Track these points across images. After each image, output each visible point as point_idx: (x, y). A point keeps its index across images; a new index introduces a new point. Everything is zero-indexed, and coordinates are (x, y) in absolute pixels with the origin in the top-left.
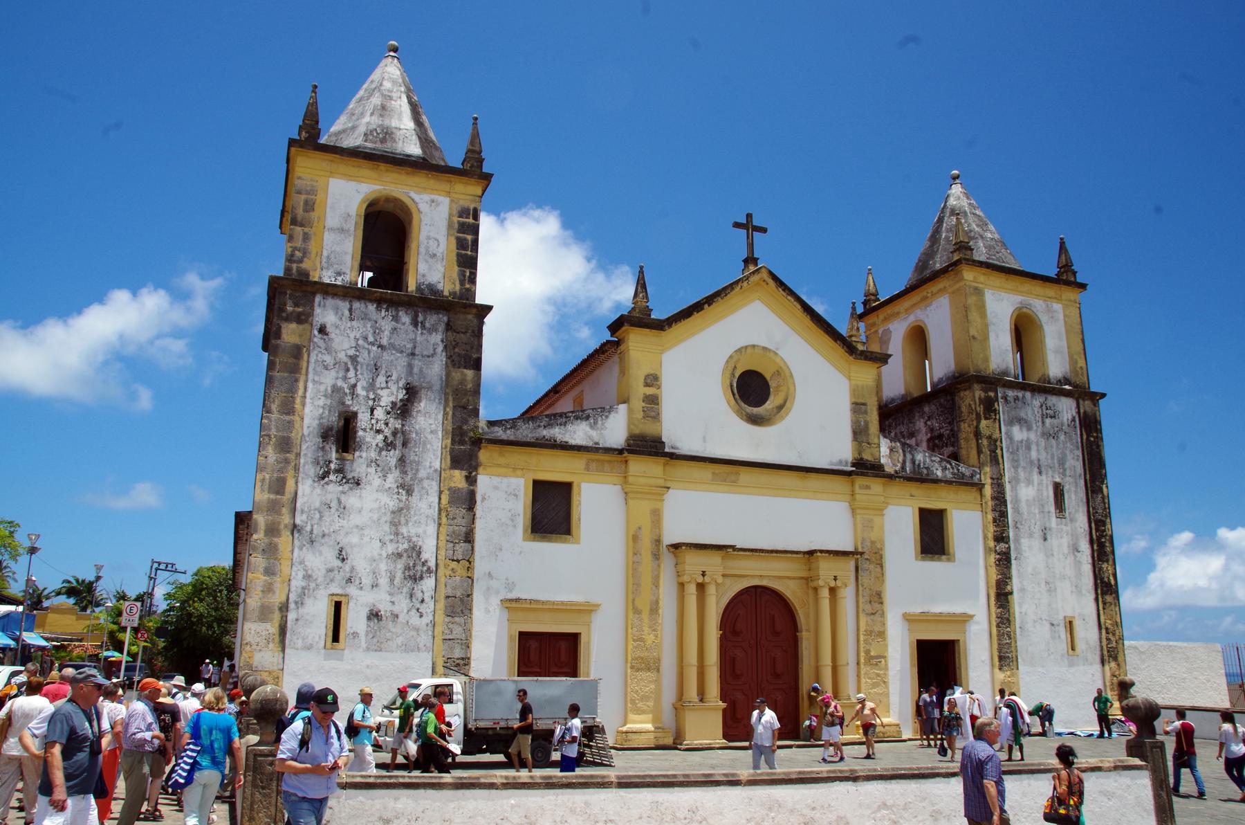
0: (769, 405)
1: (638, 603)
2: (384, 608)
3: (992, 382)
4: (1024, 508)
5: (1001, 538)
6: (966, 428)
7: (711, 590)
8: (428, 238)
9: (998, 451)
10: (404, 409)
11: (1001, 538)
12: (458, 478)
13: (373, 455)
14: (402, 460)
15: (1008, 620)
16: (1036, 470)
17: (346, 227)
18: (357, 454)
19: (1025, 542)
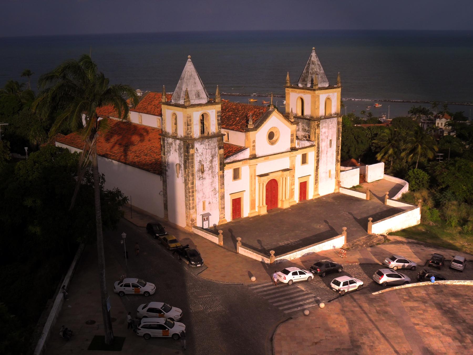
0: (274, 139)
3: (319, 119)
4: (323, 148)
5: (318, 156)
6: (312, 131)
10: (211, 161)
11: (318, 156)
13: (207, 172)
14: (212, 172)
19: (322, 156)
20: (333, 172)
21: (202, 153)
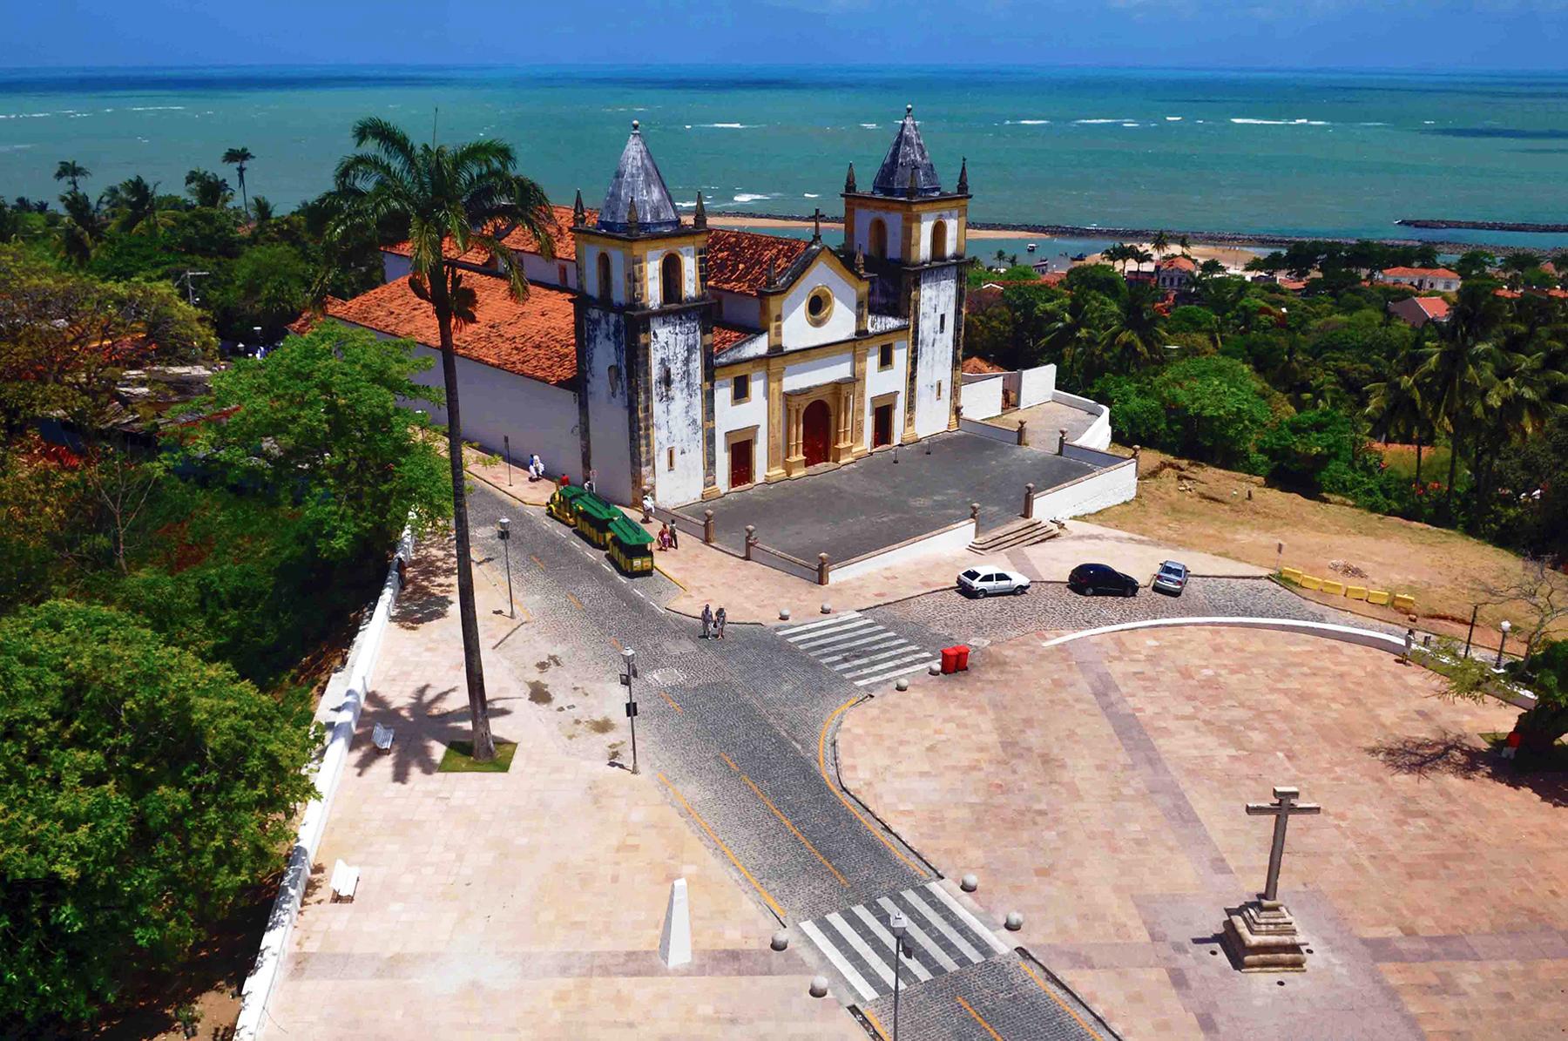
10: (687, 361)
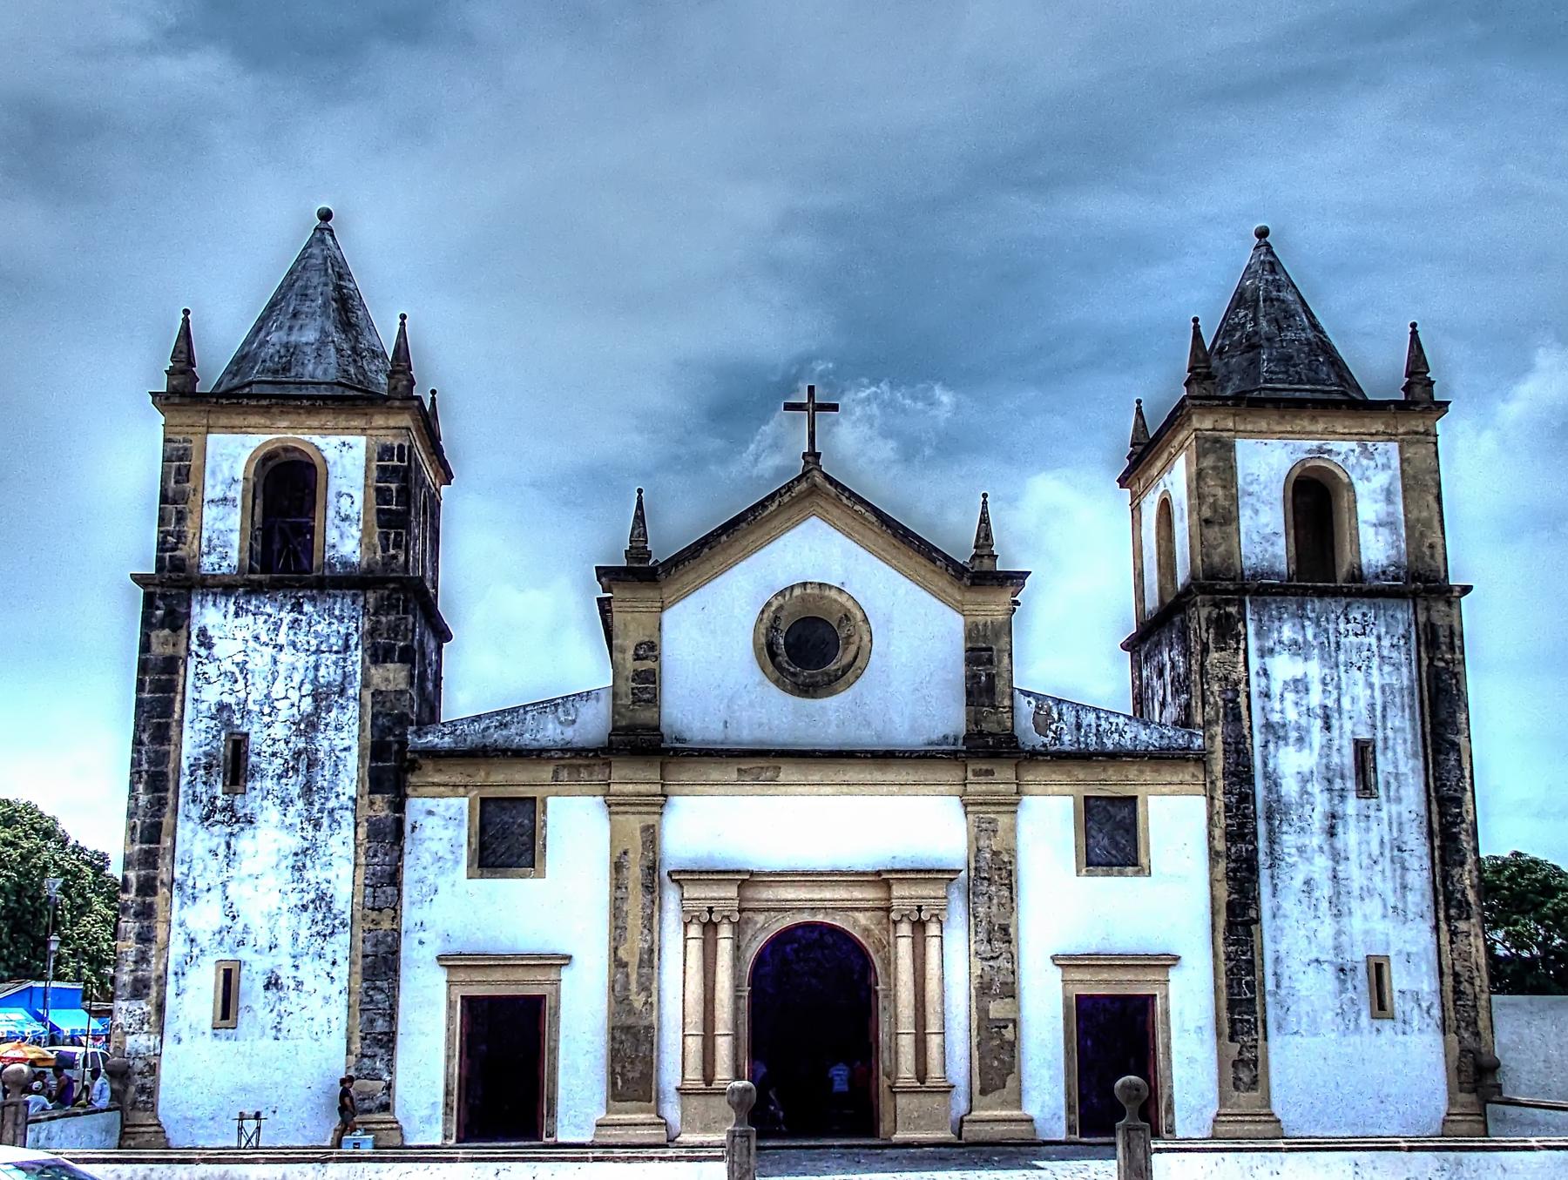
0: (832, 667)
1: (621, 953)
2: (286, 974)
7: (725, 931)
8: (340, 495)
9: (1242, 700)
12: (381, 808)
14: (308, 790)
15: (1251, 962)
16: (1319, 723)
17: (230, 495)
18: (250, 785)
19: (1289, 840)
20: (1414, 981)
21: (242, 667)
